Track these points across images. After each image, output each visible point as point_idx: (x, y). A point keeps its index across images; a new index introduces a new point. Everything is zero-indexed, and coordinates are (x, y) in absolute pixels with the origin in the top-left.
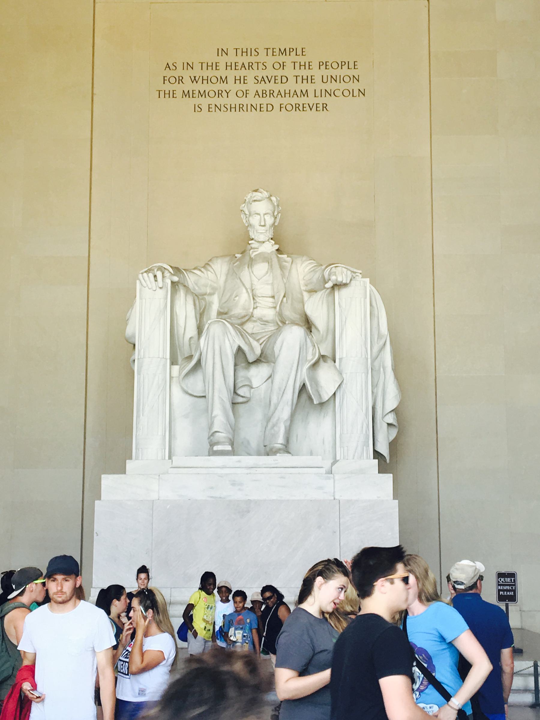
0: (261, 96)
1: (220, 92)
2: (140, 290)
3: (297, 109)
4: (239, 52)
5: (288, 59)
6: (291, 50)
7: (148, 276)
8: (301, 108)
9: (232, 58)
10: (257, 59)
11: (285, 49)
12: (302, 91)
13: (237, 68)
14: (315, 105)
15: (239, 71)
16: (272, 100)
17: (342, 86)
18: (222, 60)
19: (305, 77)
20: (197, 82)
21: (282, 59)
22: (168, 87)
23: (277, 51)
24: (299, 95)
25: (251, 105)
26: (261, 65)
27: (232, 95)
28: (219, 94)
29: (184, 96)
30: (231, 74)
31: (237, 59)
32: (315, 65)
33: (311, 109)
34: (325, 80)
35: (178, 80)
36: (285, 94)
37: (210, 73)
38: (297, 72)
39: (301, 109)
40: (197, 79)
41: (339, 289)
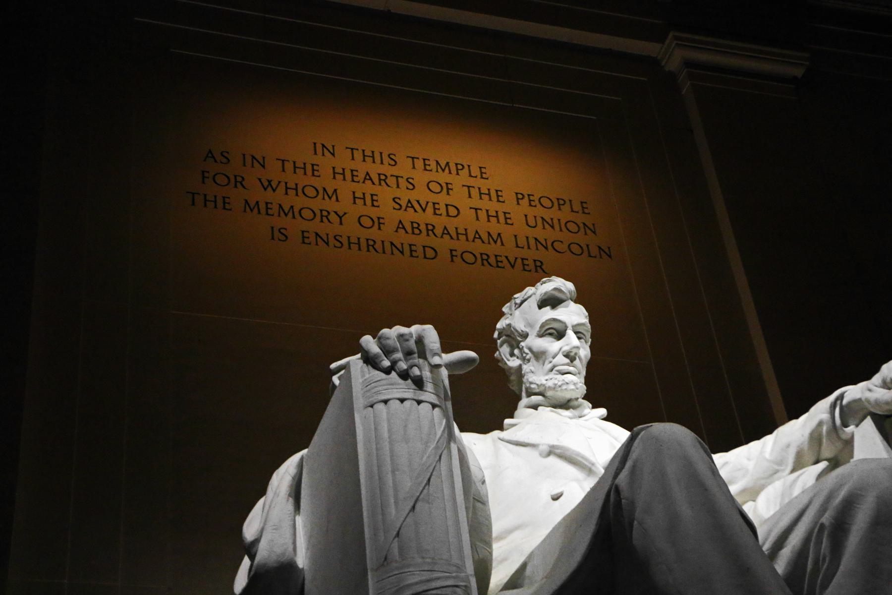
0: (409, 229)
4: (358, 155)
5: (458, 181)
6: (459, 167)
8: (492, 260)
9: (343, 161)
10: (394, 171)
13: (356, 179)
14: (519, 261)
15: (361, 184)
18: (326, 163)
20: (274, 191)
21: (443, 177)
23: (433, 165)
24: (486, 241)
28: (325, 216)
29: (248, 209)
30: (345, 189)
32: (508, 196)
33: (513, 267)
34: (532, 223)
35: (233, 180)
36: (458, 234)
38: (475, 202)
39: (495, 265)
40: (274, 184)
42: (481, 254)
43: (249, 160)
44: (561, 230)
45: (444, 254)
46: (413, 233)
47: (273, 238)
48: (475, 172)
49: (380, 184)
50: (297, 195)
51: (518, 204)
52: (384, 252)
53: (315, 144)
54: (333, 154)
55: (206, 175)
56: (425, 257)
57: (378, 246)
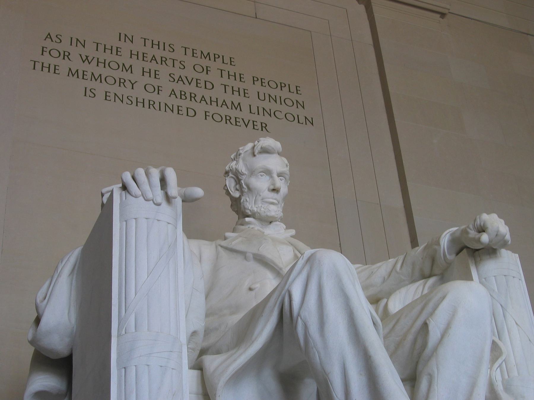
1: (122, 81)
2: (122, 205)
3: (228, 121)
7: (147, 174)
9: (138, 46)
10: (173, 55)
11: (209, 54)
12: (232, 102)
14: (251, 122)
15: (148, 63)
16: (193, 105)
17: (284, 108)
18: (126, 47)
19: (236, 89)
20: (89, 63)
21: (205, 62)
22: (47, 59)
23: (199, 54)
25: (166, 104)
26: (177, 64)
27: (139, 87)
28: (122, 82)
30: (138, 65)
31: (145, 50)
32: (248, 79)
33: (246, 126)
34: (262, 97)
36: (211, 101)
37: (108, 57)
41: (477, 264)
42: (226, 116)
43: (74, 41)
44: (281, 104)
45: (201, 115)
46: (181, 98)
47: (85, 95)
48: (227, 60)
49: (162, 64)
50: (105, 67)
51: (254, 84)
52: (160, 110)
53: (120, 34)
54: (132, 42)
55: (45, 49)
56: (188, 115)
57: (157, 106)
